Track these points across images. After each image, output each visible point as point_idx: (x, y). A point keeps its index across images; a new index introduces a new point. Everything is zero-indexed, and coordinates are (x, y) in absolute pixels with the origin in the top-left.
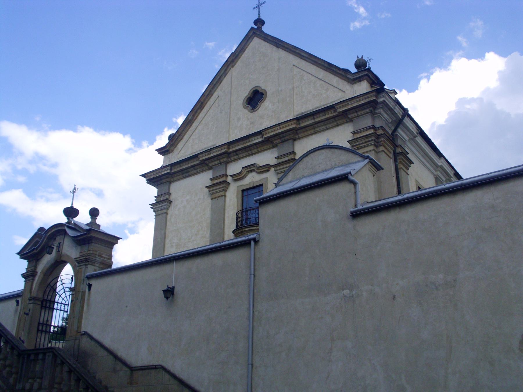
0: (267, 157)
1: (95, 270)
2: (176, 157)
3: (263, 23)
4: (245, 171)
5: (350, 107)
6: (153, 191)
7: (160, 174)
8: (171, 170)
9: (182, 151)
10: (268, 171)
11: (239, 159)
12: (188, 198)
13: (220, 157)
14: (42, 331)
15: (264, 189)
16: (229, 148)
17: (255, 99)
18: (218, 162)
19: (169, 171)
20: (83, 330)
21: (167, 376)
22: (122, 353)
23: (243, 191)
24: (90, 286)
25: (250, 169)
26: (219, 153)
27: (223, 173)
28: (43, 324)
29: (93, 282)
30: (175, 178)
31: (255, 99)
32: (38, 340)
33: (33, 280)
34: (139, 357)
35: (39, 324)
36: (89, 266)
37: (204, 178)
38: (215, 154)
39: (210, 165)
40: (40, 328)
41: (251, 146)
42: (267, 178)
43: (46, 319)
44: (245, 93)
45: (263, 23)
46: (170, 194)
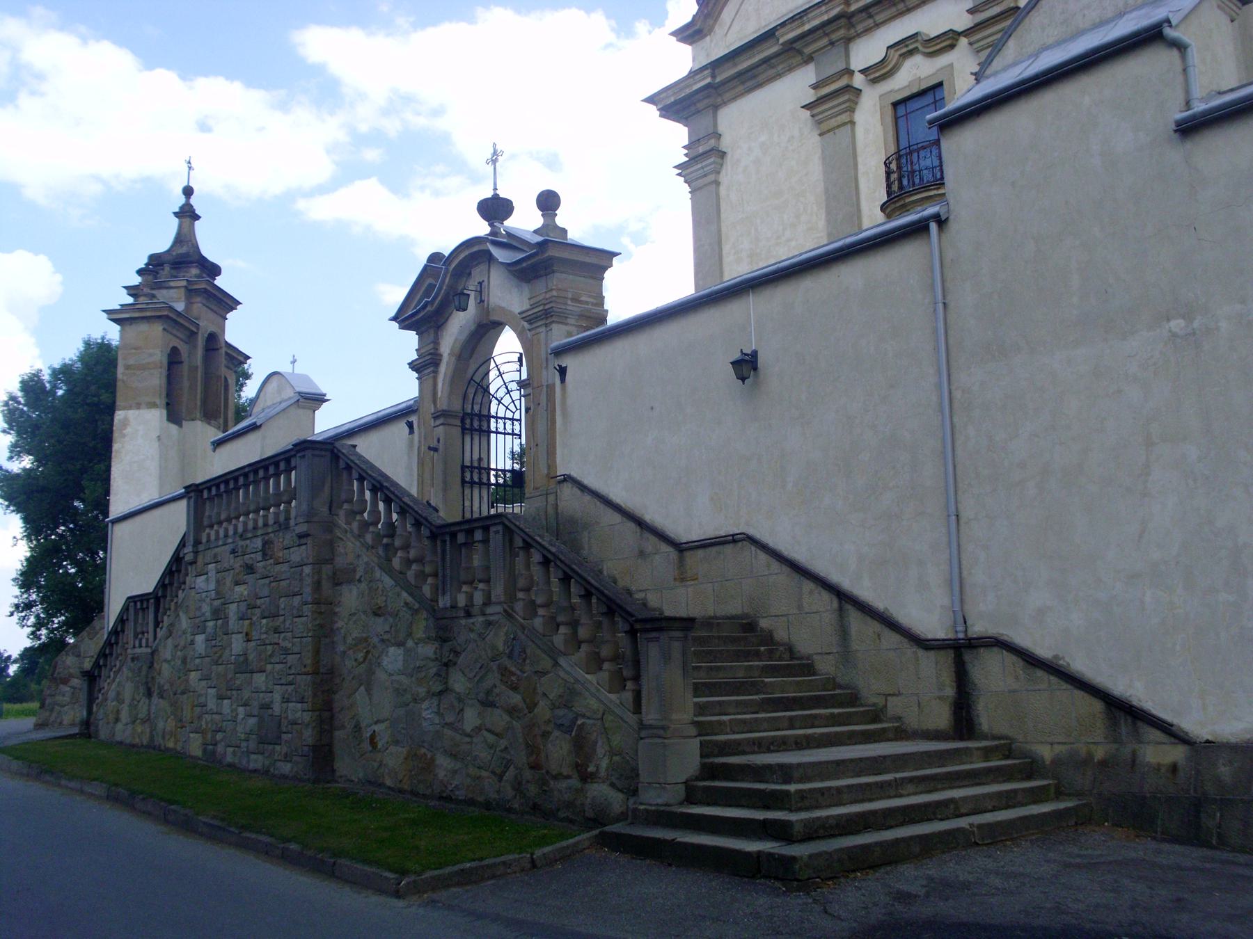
1: (570, 334)
2: (723, 41)
4: (895, 56)
6: (676, 135)
7: (688, 91)
8: (713, 77)
9: (735, 28)
10: (952, 46)
11: (878, 25)
12: (763, 138)
13: (828, 29)
14: (472, 483)
15: (946, 93)
18: (825, 41)
19: (709, 80)
21: (762, 556)
22: (652, 515)
23: (895, 105)
24: (563, 371)
25: (907, 47)
26: (825, 18)
27: (842, 66)
28: (472, 467)
29: (567, 361)
30: (727, 96)
32: (467, 503)
33: (436, 372)
34: (691, 518)
35: (463, 468)
36: (554, 326)
37: (797, 86)
38: (816, 22)
39: (807, 51)
42: (951, 65)
43: (476, 456)
46: (718, 136)
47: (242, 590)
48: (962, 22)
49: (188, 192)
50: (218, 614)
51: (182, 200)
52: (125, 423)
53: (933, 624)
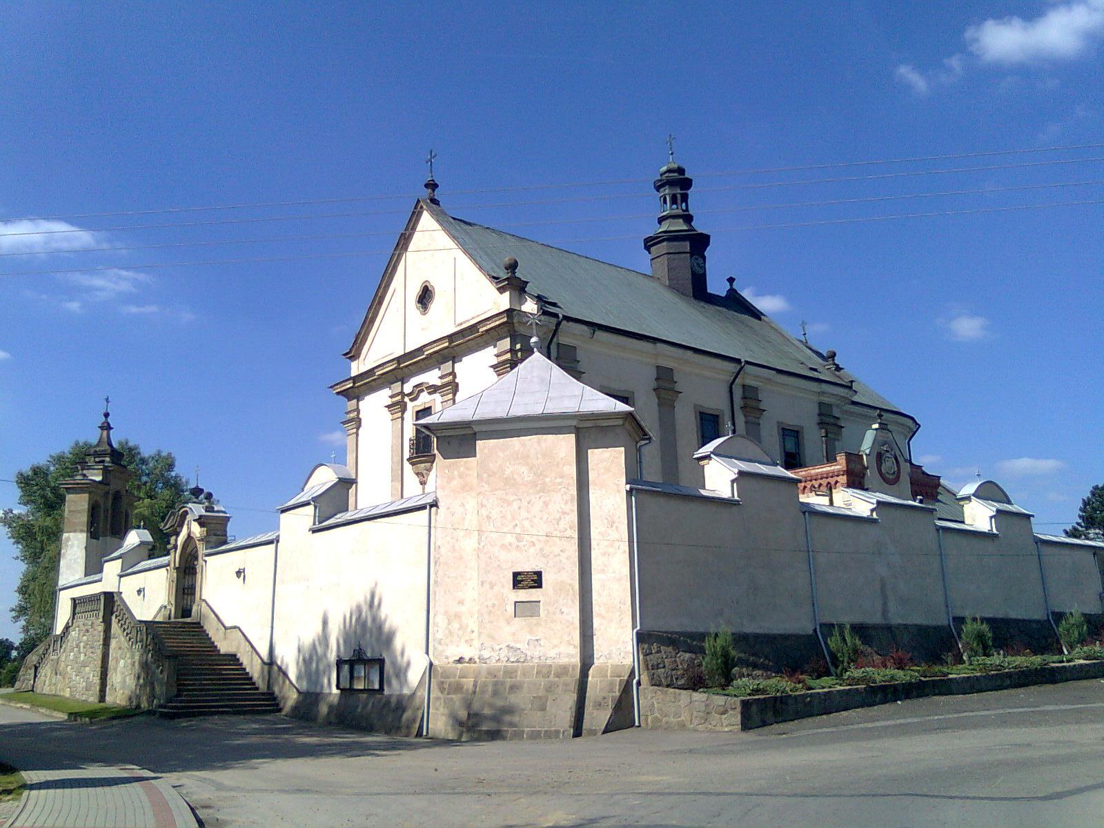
0: (432, 377)
5: (488, 327)
8: (354, 383)
10: (434, 392)
16: (399, 364)
17: (425, 297)
20: (203, 598)
25: (419, 389)
29: (206, 558)
31: (425, 297)
32: (185, 602)
40: (186, 591)
41: (418, 361)
44: (414, 291)
47: (85, 638)
48: (439, 383)
49: (107, 415)
50: (78, 646)
51: (104, 419)
52: (68, 539)
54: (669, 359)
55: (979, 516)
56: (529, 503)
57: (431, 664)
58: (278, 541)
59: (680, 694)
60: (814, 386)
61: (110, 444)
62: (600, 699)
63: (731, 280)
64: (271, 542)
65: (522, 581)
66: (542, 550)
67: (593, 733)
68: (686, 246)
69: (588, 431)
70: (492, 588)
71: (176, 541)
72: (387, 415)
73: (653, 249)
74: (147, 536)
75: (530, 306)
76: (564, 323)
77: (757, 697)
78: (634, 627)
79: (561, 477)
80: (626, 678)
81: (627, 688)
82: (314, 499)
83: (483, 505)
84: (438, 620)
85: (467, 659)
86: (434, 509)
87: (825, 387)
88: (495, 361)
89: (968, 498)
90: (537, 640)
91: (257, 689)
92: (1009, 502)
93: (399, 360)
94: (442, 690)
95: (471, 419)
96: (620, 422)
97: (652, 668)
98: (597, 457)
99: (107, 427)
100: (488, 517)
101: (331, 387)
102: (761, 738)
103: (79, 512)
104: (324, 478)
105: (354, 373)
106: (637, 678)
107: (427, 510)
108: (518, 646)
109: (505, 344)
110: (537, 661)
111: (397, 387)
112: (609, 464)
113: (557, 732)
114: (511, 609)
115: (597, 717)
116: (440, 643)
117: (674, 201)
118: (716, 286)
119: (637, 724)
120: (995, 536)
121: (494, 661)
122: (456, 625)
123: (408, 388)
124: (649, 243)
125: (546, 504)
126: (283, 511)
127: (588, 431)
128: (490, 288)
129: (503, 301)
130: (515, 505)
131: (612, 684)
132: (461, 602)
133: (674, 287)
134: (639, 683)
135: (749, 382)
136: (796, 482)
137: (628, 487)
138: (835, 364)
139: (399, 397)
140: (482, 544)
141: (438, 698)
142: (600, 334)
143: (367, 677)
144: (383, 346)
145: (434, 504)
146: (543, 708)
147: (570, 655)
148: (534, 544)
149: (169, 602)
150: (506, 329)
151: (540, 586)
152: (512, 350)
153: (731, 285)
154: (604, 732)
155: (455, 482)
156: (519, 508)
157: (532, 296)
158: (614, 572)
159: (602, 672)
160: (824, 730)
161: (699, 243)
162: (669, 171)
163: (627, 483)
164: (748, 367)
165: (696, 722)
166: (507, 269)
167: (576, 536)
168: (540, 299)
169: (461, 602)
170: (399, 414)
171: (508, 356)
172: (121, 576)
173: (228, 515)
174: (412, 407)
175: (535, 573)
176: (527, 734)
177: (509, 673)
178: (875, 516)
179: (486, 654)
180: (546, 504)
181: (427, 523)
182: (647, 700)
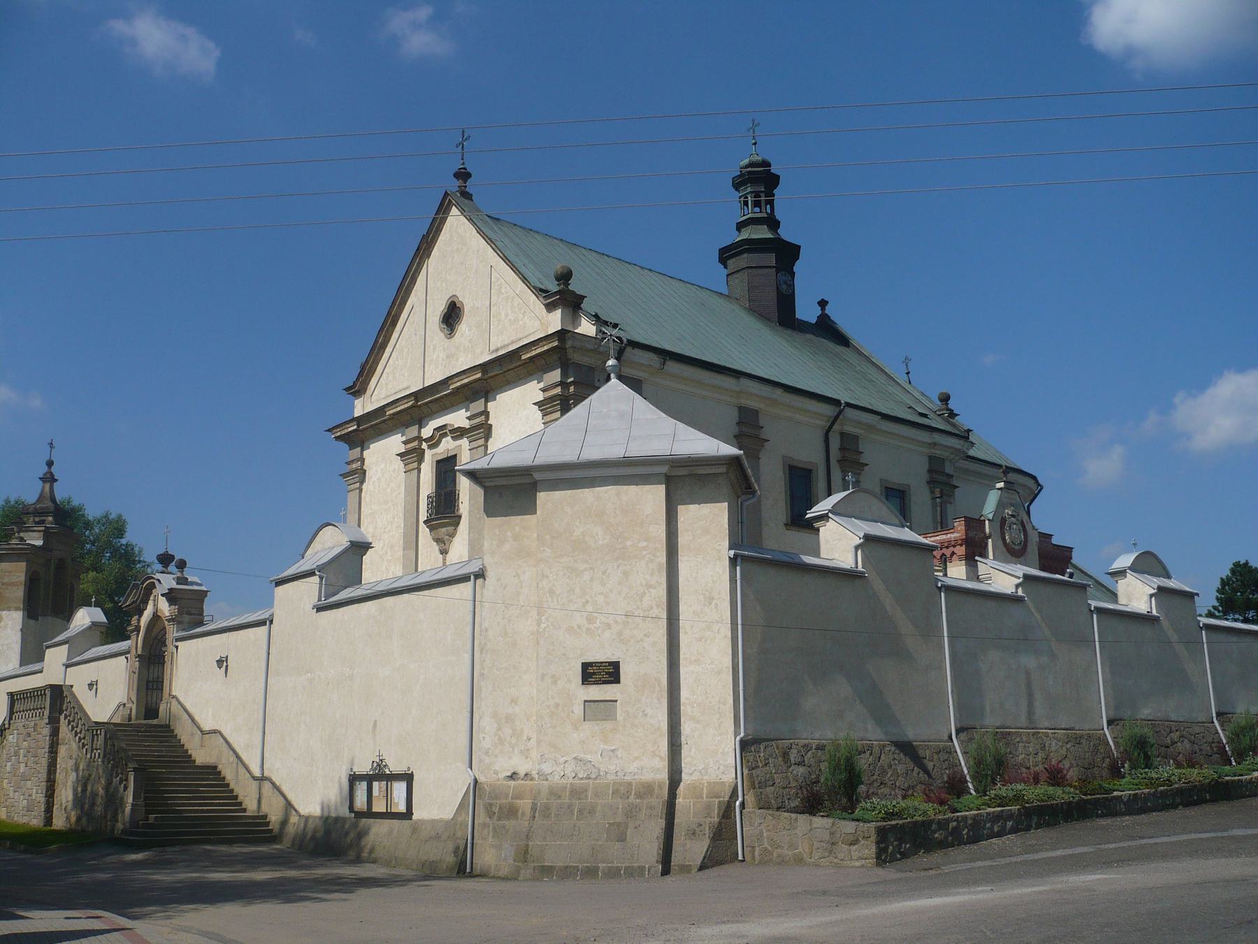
0: (459, 418)
3: (468, 175)
5: (534, 353)
8: (359, 426)
16: (417, 401)
17: (452, 316)
23: (438, 462)
25: (442, 431)
29: (178, 644)
31: (452, 316)
37: (394, 443)
44: (439, 308)
45: (468, 175)
48: (466, 424)
49: (50, 464)
50: (16, 754)
51: (46, 469)
53: (257, 773)
54: (755, 397)
55: (1136, 595)
56: (604, 573)
57: (476, 781)
58: (271, 622)
59: (796, 820)
60: (924, 436)
61: (53, 499)
62: (694, 826)
63: (823, 304)
64: (261, 623)
65: (594, 674)
66: (620, 633)
67: (685, 869)
68: (771, 259)
69: (682, 479)
70: (555, 683)
71: (139, 621)
72: (399, 464)
73: (730, 262)
74: (98, 615)
75: (587, 328)
76: (629, 349)
77: (893, 822)
78: (736, 734)
79: (647, 540)
80: (727, 799)
81: (727, 812)
82: (322, 568)
83: (544, 576)
84: (485, 723)
85: (522, 773)
86: (479, 581)
87: (938, 438)
88: (540, 397)
89: (1121, 573)
90: (613, 751)
91: (245, 810)
92: (1168, 577)
93: (416, 395)
94: (490, 814)
95: (530, 463)
96: (723, 469)
97: (755, 784)
98: (689, 514)
99: (49, 479)
100: (551, 592)
101: (329, 430)
102: (903, 875)
103: (13, 584)
104: (330, 542)
105: (358, 412)
106: (740, 799)
107: (470, 585)
108: (589, 757)
109: (555, 376)
110: (613, 777)
111: (412, 431)
112: (707, 524)
113: (642, 869)
114: (578, 710)
115: (690, 850)
116: (487, 753)
117: (757, 204)
118: (806, 311)
119: (740, 858)
120: (1156, 619)
121: (557, 777)
122: (508, 731)
123: (427, 432)
124: (726, 255)
125: (626, 574)
126: (279, 583)
127: (682, 479)
128: (537, 304)
129: (554, 321)
130: (586, 576)
131: (709, 806)
132: (514, 701)
133: (756, 310)
134: (743, 805)
135: (849, 429)
136: (929, 549)
137: (732, 553)
138: (948, 409)
139: (415, 444)
140: (543, 626)
141: (485, 825)
142: (672, 367)
143: (388, 795)
144: (395, 379)
145: (480, 575)
146: (622, 838)
147: (655, 769)
148: (609, 626)
149: (129, 699)
150: (555, 357)
151: (617, 681)
152: (562, 384)
153: (823, 309)
154: (701, 868)
155: (507, 547)
156: (592, 580)
157: (589, 315)
158: (712, 663)
159: (695, 789)
160: (979, 864)
161: (787, 254)
162: (751, 165)
163: (730, 549)
164: (849, 411)
165: (817, 855)
166: (558, 279)
167: (664, 615)
168: (597, 319)
169: (514, 701)
170: (415, 465)
171: (558, 390)
172: (67, 666)
173: (203, 588)
174: (430, 457)
175: (611, 663)
176: (603, 873)
177: (578, 792)
178: (1020, 592)
179: (547, 768)
180: (626, 574)
181: (471, 597)
182: (754, 827)
